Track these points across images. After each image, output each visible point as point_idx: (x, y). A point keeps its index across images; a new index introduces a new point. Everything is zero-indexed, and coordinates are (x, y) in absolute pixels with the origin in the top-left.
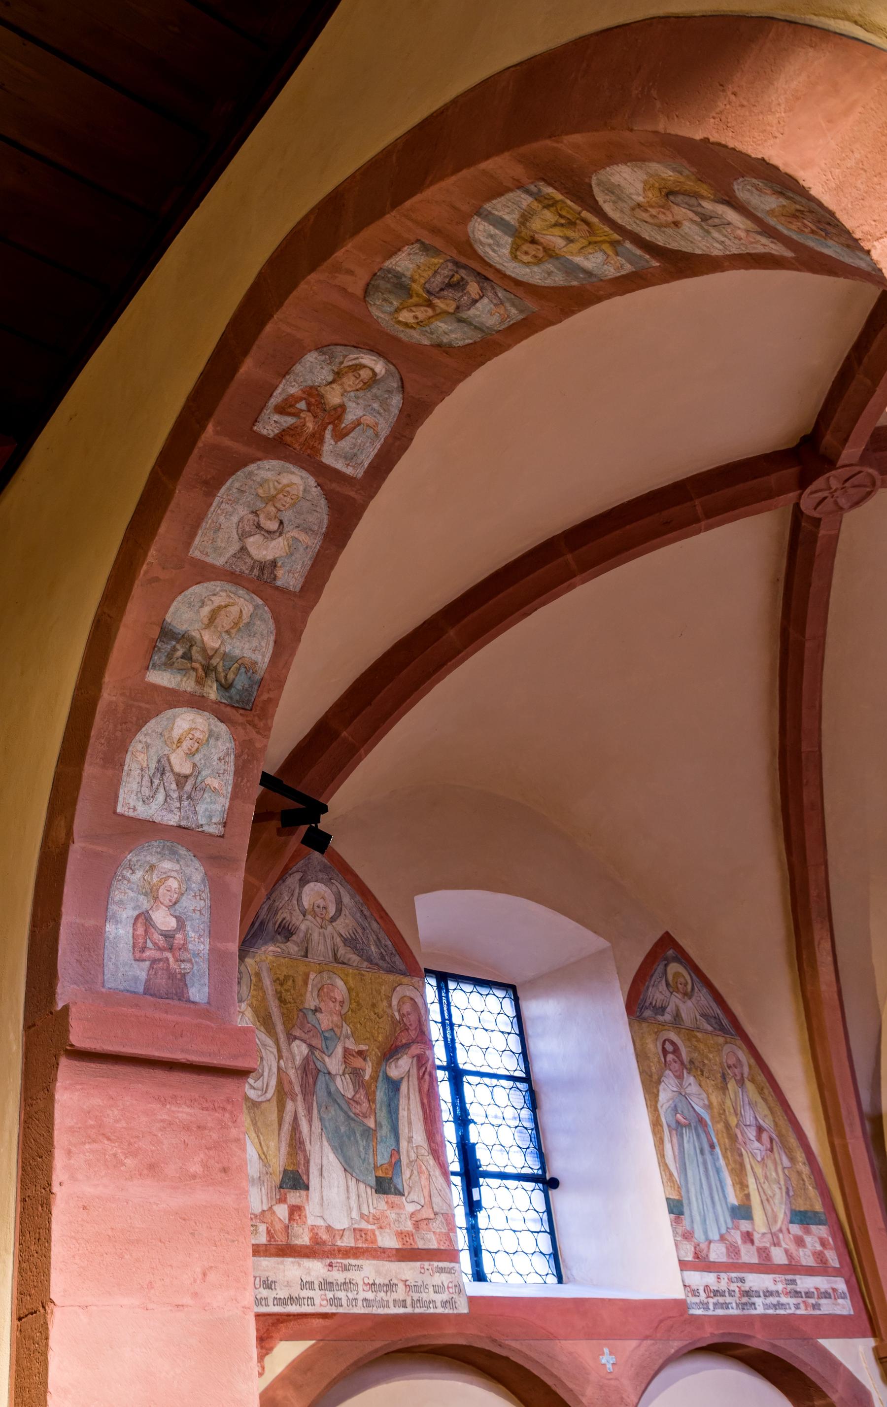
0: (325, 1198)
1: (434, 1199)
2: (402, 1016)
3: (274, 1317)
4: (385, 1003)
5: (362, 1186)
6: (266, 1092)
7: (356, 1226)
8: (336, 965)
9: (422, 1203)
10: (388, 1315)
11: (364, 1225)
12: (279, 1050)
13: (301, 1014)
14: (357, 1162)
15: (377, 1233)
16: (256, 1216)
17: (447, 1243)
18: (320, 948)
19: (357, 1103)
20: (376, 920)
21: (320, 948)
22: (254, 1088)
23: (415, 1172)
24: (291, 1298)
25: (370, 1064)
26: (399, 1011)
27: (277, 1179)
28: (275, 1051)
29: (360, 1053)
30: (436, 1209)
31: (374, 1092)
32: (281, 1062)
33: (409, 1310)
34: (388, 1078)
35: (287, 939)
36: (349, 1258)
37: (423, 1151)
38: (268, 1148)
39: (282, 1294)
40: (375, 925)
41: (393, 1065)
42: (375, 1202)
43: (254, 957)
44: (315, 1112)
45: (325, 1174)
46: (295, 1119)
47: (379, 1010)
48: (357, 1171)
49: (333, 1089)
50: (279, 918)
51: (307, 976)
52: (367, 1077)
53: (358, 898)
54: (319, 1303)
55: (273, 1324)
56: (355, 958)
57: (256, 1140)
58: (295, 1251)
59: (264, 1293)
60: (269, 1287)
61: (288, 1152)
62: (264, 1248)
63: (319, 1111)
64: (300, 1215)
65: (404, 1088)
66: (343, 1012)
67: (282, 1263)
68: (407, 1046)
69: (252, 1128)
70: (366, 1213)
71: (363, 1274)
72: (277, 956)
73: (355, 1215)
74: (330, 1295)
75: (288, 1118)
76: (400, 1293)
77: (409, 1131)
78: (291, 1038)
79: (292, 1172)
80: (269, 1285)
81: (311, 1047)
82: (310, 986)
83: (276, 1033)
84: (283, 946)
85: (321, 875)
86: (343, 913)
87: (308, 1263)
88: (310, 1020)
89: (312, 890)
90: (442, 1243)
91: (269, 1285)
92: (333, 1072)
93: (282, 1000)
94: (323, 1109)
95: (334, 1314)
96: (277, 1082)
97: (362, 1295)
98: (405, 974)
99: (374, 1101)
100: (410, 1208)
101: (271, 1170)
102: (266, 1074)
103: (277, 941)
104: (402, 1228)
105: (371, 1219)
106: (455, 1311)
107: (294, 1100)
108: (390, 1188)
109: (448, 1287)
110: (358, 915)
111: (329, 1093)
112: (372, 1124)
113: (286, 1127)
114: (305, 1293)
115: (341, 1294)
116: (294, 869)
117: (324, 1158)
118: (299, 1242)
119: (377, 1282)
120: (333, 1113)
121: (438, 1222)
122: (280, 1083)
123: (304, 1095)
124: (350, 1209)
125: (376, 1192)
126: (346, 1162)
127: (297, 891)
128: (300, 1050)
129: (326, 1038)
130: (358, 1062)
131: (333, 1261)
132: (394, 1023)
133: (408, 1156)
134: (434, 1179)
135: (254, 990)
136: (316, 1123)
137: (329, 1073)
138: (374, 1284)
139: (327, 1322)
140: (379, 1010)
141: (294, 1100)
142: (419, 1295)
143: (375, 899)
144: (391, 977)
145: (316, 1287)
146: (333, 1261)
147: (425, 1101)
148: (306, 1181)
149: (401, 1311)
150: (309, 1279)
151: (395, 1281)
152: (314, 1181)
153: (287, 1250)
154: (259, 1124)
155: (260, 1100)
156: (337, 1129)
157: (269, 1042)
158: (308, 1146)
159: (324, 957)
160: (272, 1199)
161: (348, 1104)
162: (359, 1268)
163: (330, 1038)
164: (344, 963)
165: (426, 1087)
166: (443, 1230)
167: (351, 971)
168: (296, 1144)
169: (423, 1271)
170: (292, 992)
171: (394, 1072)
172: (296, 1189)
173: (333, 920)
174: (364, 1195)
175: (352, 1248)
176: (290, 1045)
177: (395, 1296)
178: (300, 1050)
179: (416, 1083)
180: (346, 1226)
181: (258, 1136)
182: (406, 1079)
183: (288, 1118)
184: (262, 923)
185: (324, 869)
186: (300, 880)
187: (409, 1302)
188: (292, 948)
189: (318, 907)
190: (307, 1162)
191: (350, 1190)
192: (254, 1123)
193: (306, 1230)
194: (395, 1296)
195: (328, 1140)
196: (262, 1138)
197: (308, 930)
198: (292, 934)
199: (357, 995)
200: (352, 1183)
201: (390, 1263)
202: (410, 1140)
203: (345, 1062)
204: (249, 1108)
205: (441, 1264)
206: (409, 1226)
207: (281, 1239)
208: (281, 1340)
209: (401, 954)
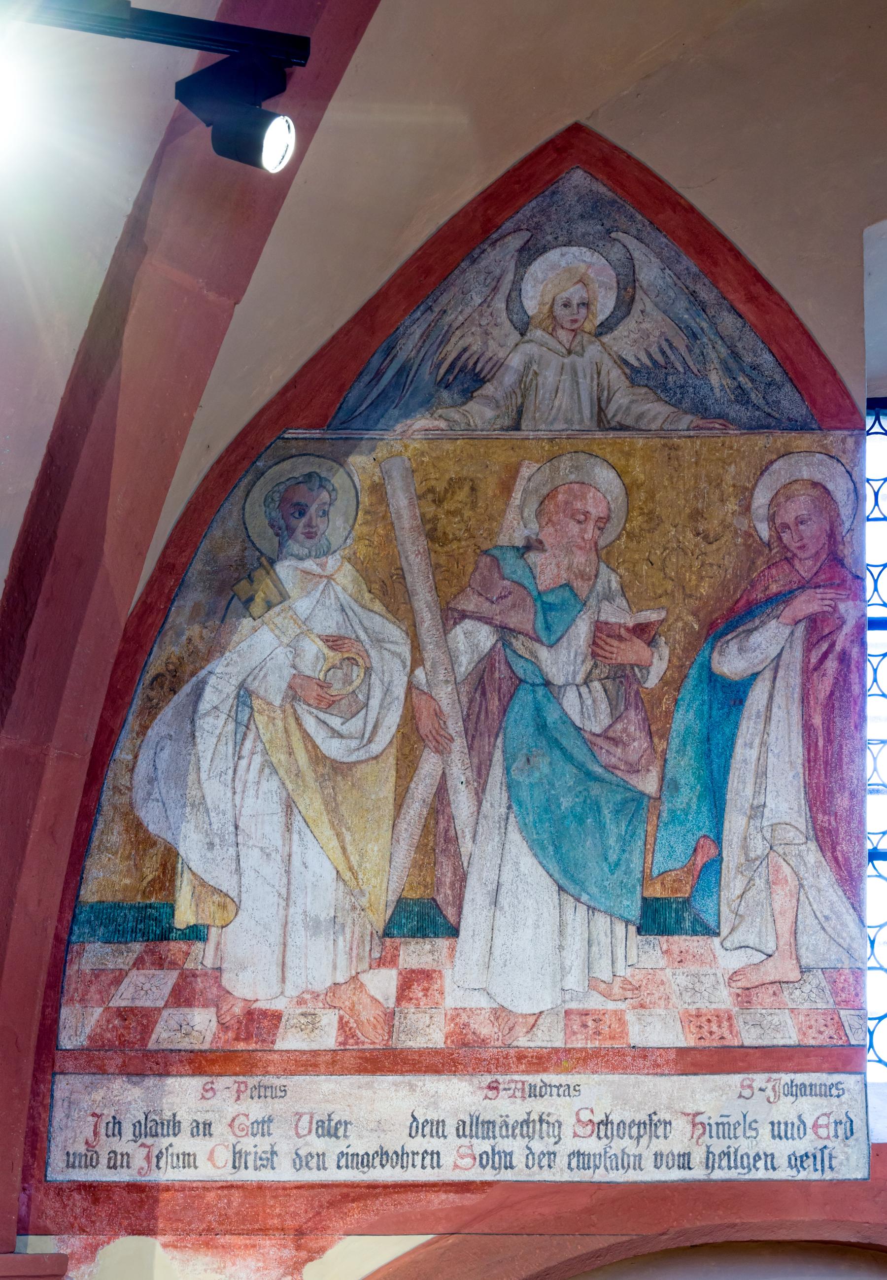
0: (497, 952)
1: (803, 939)
2: (779, 529)
3: (336, 1191)
4: (732, 506)
5: (602, 921)
6: (370, 741)
7: (573, 1005)
8: (599, 435)
9: (770, 947)
10: (635, 1183)
11: (595, 1002)
12: (416, 647)
13: (485, 560)
14: (595, 870)
15: (630, 1017)
16: (316, 996)
17: (830, 1031)
18: (560, 398)
19: (615, 741)
20: (733, 309)
21: (560, 398)
22: (341, 736)
23: (760, 883)
24: (383, 1154)
25: (666, 652)
26: (771, 519)
27: (379, 919)
28: (406, 651)
29: (641, 630)
30: (807, 959)
31: (669, 715)
32: (420, 673)
33: (698, 1173)
34: (712, 679)
35: (468, 395)
36: (545, 1070)
37: (791, 834)
38: (362, 856)
39: (360, 1146)
40: (728, 322)
41: (733, 647)
42: (633, 953)
43: (373, 449)
44: (497, 772)
45: (505, 900)
46: (442, 792)
47: (713, 525)
48: (594, 890)
49: (552, 716)
50: (452, 350)
51: (513, 472)
52: (652, 681)
53: (688, 263)
54: (456, 1161)
55: (331, 1204)
56: (656, 411)
57: (335, 843)
58: (405, 1061)
59: (318, 1144)
60: (332, 1133)
61: (415, 861)
62: (329, 1057)
63: (507, 770)
64: (426, 990)
65: (757, 697)
66: (601, 543)
67: (369, 1086)
68: (785, 597)
69: (325, 818)
70: (606, 976)
71: (577, 1103)
72: (433, 437)
73: (574, 981)
74: (484, 1146)
75: (422, 789)
76: (679, 1139)
77: (756, 793)
78: (450, 616)
79: (417, 902)
80: (329, 1128)
81: (504, 632)
82: (517, 497)
83: (412, 610)
84: (454, 415)
85: (581, 227)
86: (637, 307)
87: (431, 1084)
88: (507, 571)
89: (553, 267)
90: (812, 1033)
91: (329, 1128)
92: (559, 680)
93: (433, 534)
94: (520, 762)
95: (485, 1185)
96: (403, 717)
97: (569, 1144)
98: (802, 427)
99: (664, 735)
100: (732, 961)
101: (364, 901)
102: (374, 703)
103: (439, 405)
104: (702, 1005)
105: (616, 990)
106: (828, 1176)
107: (441, 750)
108: (679, 920)
109: (816, 1126)
110: (682, 304)
111: (542, 727)
112: (649, 784)
113: (415, 810)
114: (419, 1144)
115: (516, 1146)
116: (509, 225)
117: (507, 869)
118: (418, 1043)
119: (615, 1118)
120: (546, 770)
121: (807, 988)
122: (410, 717)
123: (472, 735)
124: (563, 971)
125: (639, 931)
126: (565, 871)
127: (510, 277)
128: (473, 640)
129: (548, 608)
130: (632, 651)
131: (500, 1078)
132: (753, 546)
133: (745, 848)
134: (812, 894)
135: (366, 523)
136: (496, 794)
137: (547, 684)
138: (606, 1122)
139: (470, 1200)
140: (713, 525)
141: (441, 750)
142: (727, 1142)
143: (737, 255)
144: (761, 441)
145: (450, 1130)
146: (500, 1078)
147: (817, 721)
148: (452, 919)
149: (675, 1175)
150: (433, 1116)
151: (664, 1115)
152: (474, 917)
153: (389, 1062)
154: (343, 809)
155: (353, 758)
156: (549, 806)
157: (394, 633)
158: (466, 846)
159: (566, 421)
160: (360, 959)
161: (590, 746)
162: (570, 1090)
163: (553, 610)
164: (622, 428)
165: (823, 687)
166: (821, 1005)
167: (641, 442)
168: (438, 840)
169: (747, 1093)
170: (467, 513)
171: (731, 663)
172: (424, 936)
173: (606, 327)
174: (605, 941)
175: (556, 1050)
176: (446, 632)
177: (660, 1145)
178: (473, 640)
179: (796, 680)
180: (546, 1006)
181: (338, 835)
182: (768, 674)
183: (422, 789)
184: (403, 370)
185: (595, 208)
186: (521, 250)
187: (698, 1157)
188: (479, 413)
189: (566, 305)
190: (461, 879)
191: (569, 930)
192: (332, 808)
193: (439, 1019)
194: (660, 1145)
195: (523, 828)
196: (348, 838)
197: (527, 366)
198: (479, 380)
199: (651, 496)
200: (577, 917)
201: (658, 1079)
202: (757, 811)
203: (594, 655)
204: (321, 779)
205: (800, 1078)
206: (724, 999)
207: (372, 1039)
208: (347, 1234)
209: (797, 379)
